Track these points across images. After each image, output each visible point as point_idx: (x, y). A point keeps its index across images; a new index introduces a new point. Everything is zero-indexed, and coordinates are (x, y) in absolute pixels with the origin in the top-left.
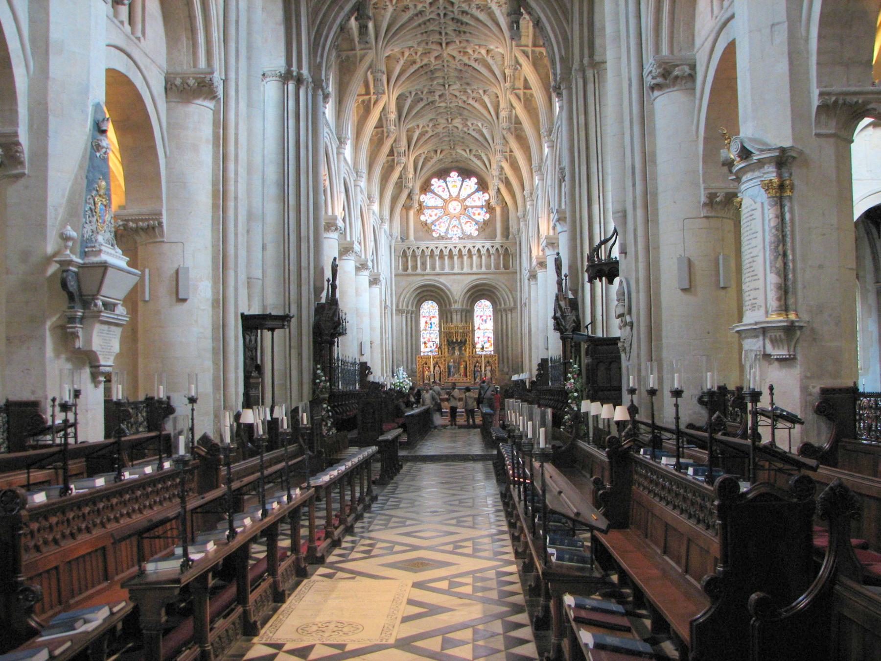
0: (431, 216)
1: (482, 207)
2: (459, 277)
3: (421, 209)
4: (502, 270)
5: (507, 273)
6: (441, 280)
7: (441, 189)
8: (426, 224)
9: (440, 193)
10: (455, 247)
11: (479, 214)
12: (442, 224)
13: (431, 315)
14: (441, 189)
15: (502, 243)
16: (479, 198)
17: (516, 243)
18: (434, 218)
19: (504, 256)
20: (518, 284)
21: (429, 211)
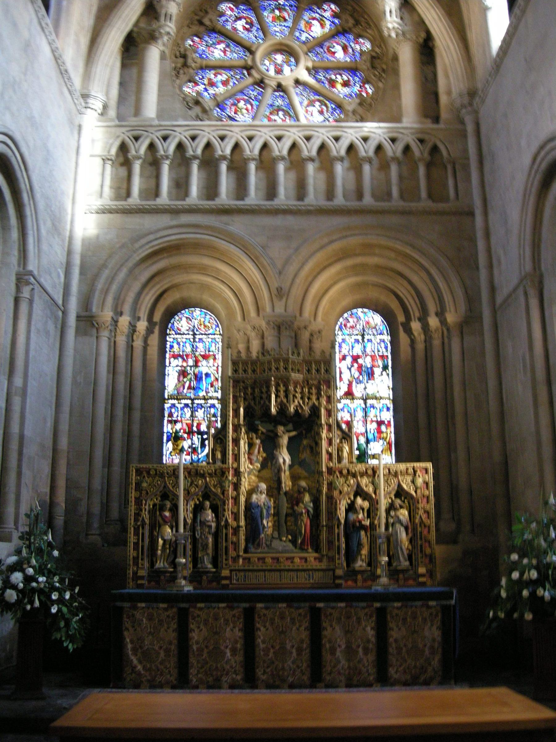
0: (212, 84)
1: (353, 70)
2: (290, 220)
3: (185, 65)
4: (425, 203)
5: (442, 213)
6: (231, 228)
7: (240, 25)
8: (197, 103)
9: (243, 34)
10: (279, 138)
11: (346, 84)
12: (242, 104)
13: (201, 349)
14: (240, 25)
15: (422, 131)
16: (345, 49)
17: (464, 135)
18: (221, 89)
19: (429, 166)
20: (481, 245)
21: (211, 75)
